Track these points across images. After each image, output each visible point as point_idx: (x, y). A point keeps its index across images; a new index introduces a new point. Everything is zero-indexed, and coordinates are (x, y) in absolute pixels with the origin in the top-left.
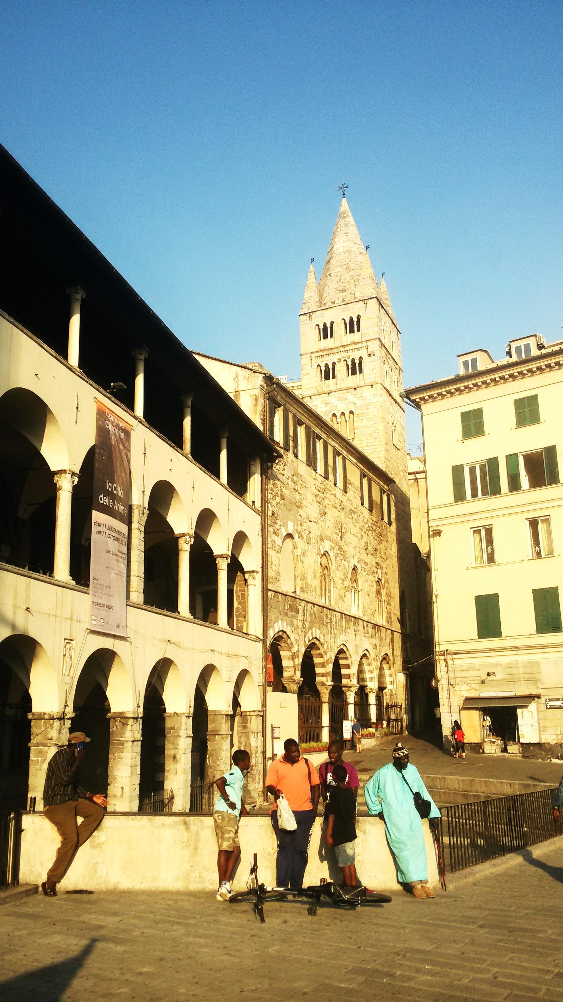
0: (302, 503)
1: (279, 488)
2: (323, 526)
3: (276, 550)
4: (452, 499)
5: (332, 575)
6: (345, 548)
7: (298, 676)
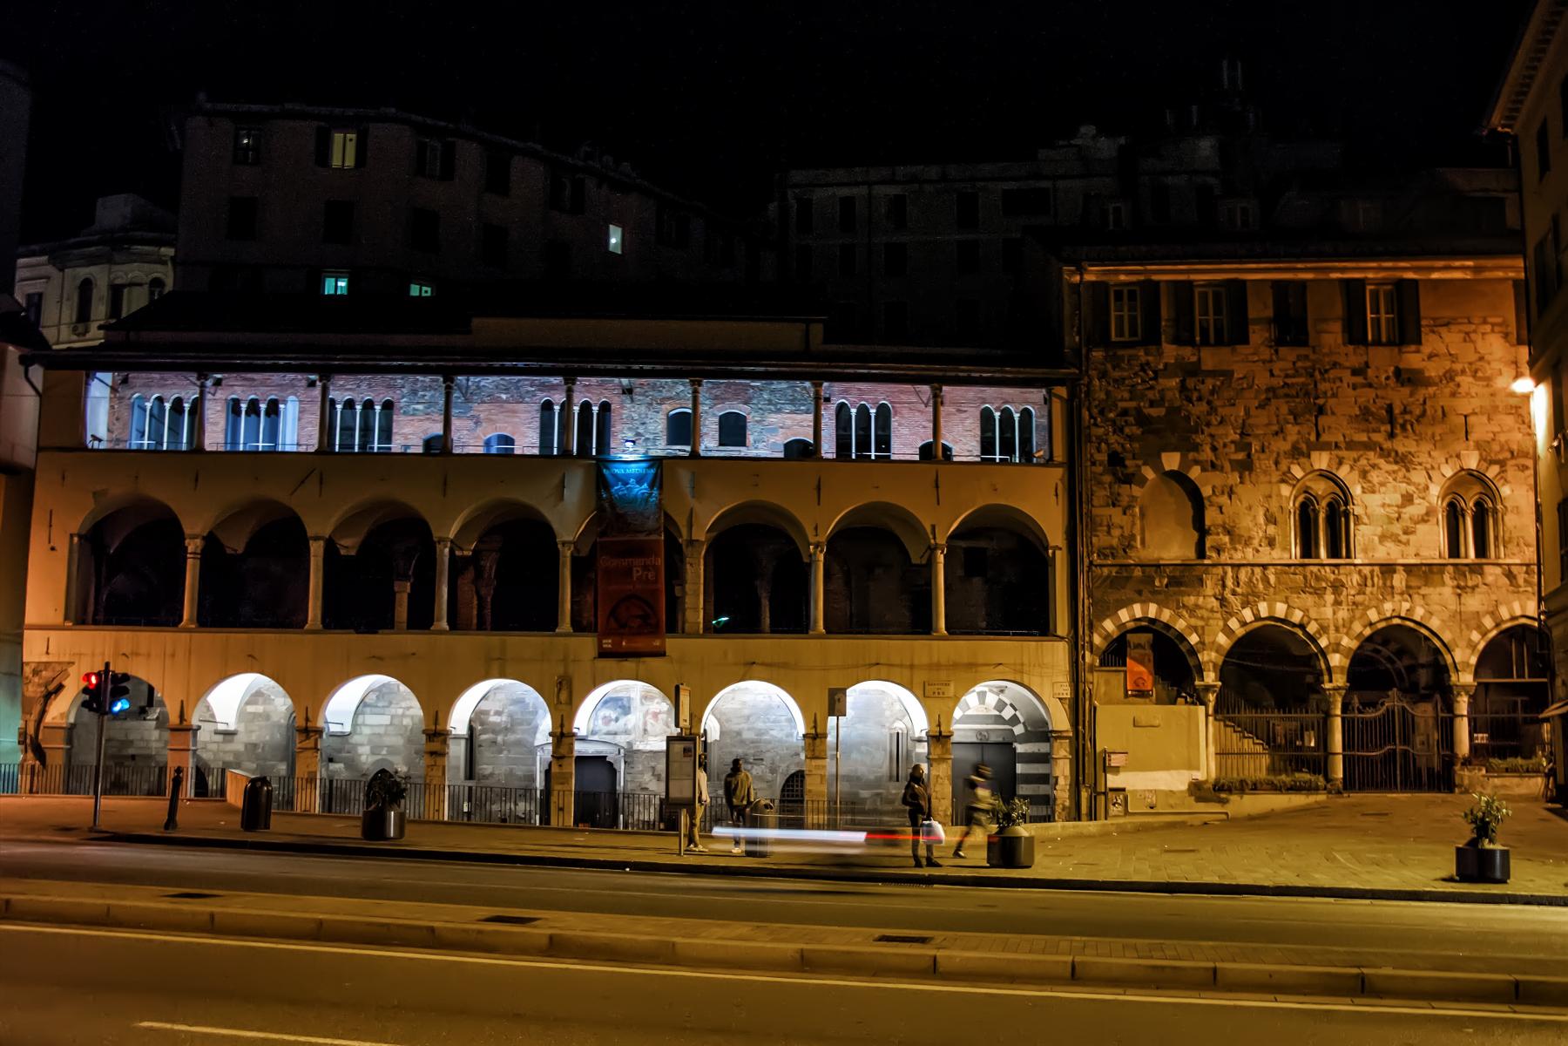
7: (1210, 677)
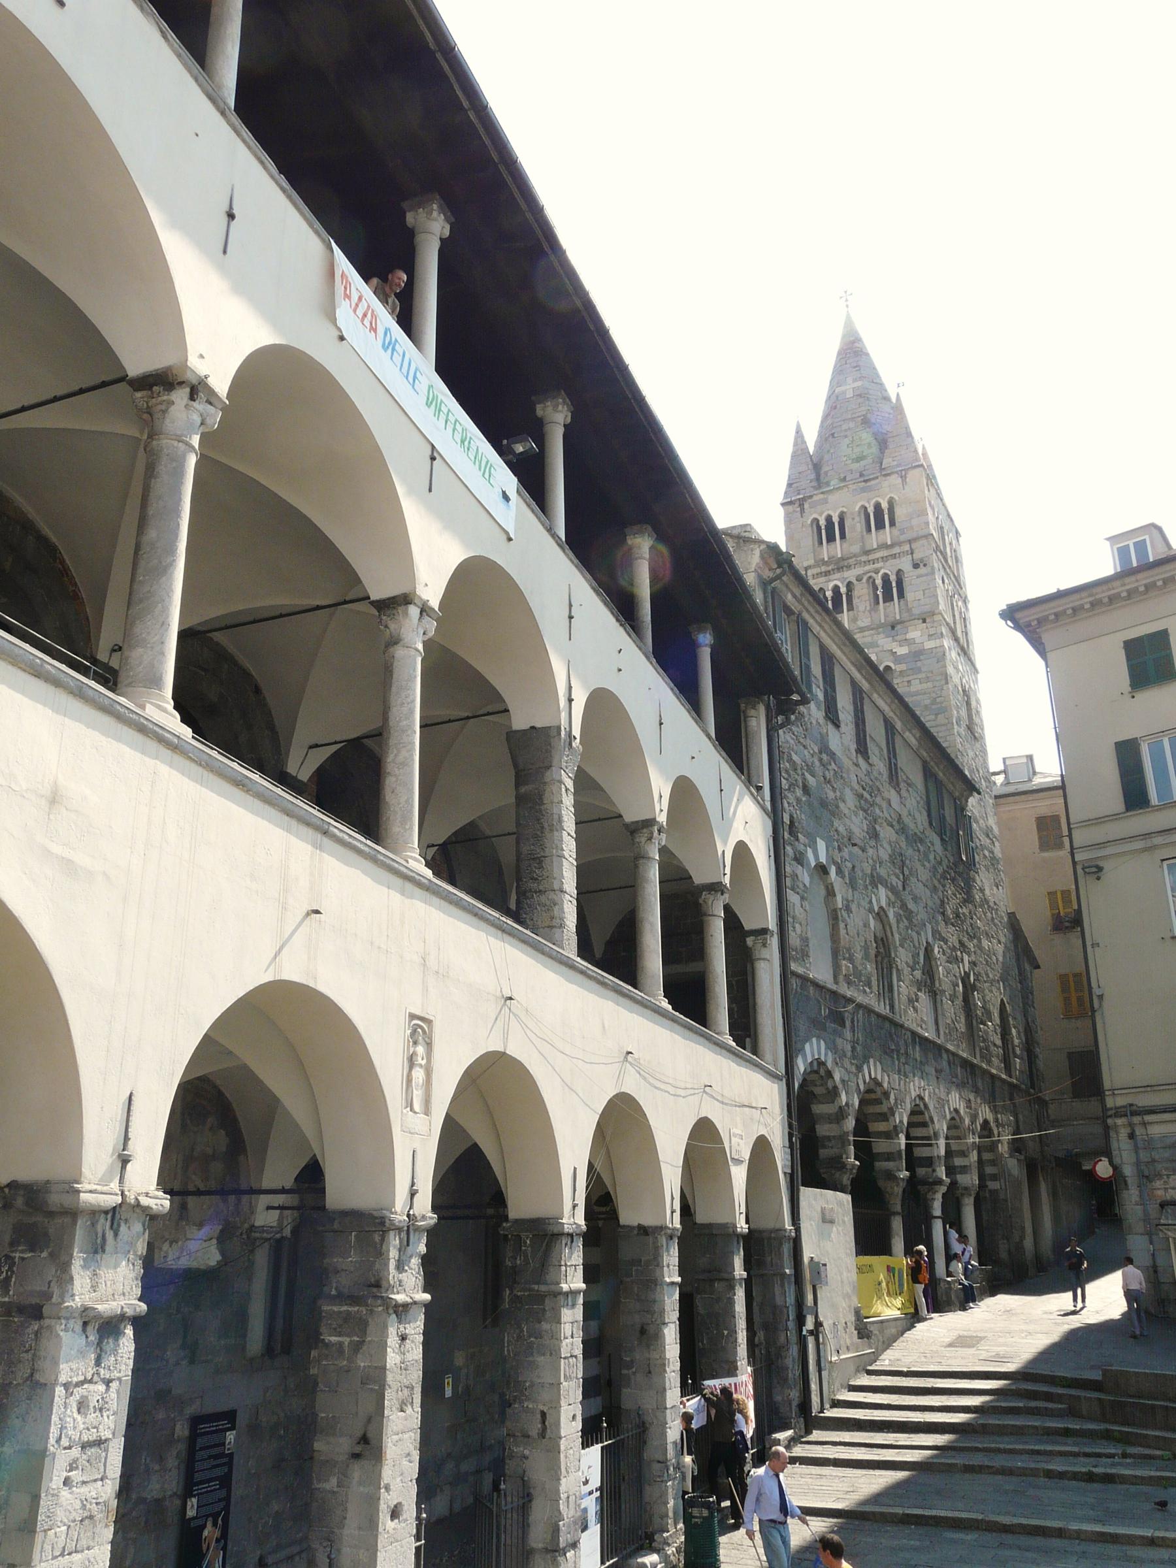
0: (837, 807)
1: (800, 773)
2: (875, 858)
3: (800, 892)
4: (1118, 804)
5: (893, 955)
6: (911, 905)
